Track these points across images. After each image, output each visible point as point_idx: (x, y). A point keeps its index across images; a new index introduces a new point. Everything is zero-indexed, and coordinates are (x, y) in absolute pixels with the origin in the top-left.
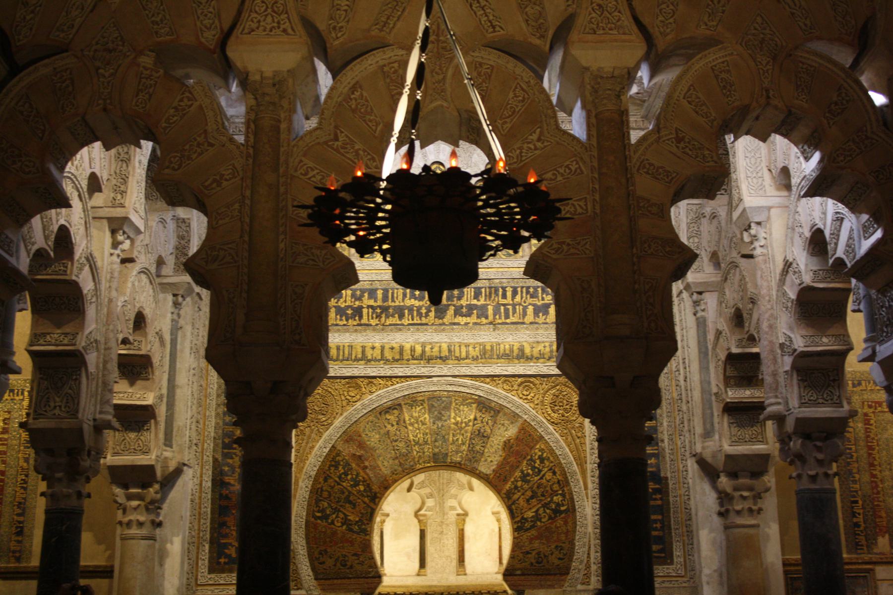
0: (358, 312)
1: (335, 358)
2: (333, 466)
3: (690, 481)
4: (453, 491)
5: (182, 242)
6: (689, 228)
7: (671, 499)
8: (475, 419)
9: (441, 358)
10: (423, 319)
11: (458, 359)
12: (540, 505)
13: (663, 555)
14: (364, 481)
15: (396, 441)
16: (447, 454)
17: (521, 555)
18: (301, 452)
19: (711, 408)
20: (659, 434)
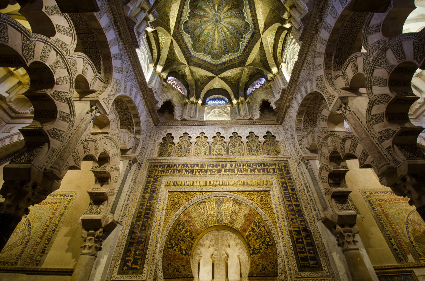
0: (192, 171)
1: (183, 185)
2: (178, 225)
3: (320, 231)
4: (224, 248)
5: (136, 146)
6: (299, 142)
7: (314, 239)
8: (232, 207)
9: (220, 185)
10: (214, 173)
11: (226, 185)
12: (261, 242)
13: (317, 266)
14: (190, 231)
15: (203, 215)
16: (222, 220)
17: (255, 266)
18: (166, 219)
19: (323, 198)
20: (303, 212)
